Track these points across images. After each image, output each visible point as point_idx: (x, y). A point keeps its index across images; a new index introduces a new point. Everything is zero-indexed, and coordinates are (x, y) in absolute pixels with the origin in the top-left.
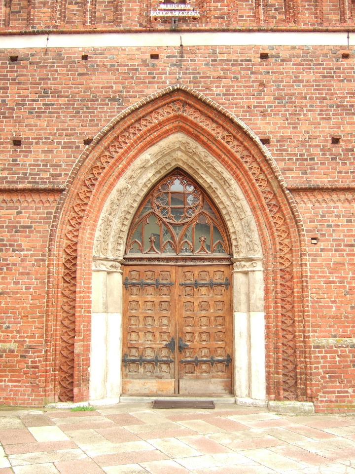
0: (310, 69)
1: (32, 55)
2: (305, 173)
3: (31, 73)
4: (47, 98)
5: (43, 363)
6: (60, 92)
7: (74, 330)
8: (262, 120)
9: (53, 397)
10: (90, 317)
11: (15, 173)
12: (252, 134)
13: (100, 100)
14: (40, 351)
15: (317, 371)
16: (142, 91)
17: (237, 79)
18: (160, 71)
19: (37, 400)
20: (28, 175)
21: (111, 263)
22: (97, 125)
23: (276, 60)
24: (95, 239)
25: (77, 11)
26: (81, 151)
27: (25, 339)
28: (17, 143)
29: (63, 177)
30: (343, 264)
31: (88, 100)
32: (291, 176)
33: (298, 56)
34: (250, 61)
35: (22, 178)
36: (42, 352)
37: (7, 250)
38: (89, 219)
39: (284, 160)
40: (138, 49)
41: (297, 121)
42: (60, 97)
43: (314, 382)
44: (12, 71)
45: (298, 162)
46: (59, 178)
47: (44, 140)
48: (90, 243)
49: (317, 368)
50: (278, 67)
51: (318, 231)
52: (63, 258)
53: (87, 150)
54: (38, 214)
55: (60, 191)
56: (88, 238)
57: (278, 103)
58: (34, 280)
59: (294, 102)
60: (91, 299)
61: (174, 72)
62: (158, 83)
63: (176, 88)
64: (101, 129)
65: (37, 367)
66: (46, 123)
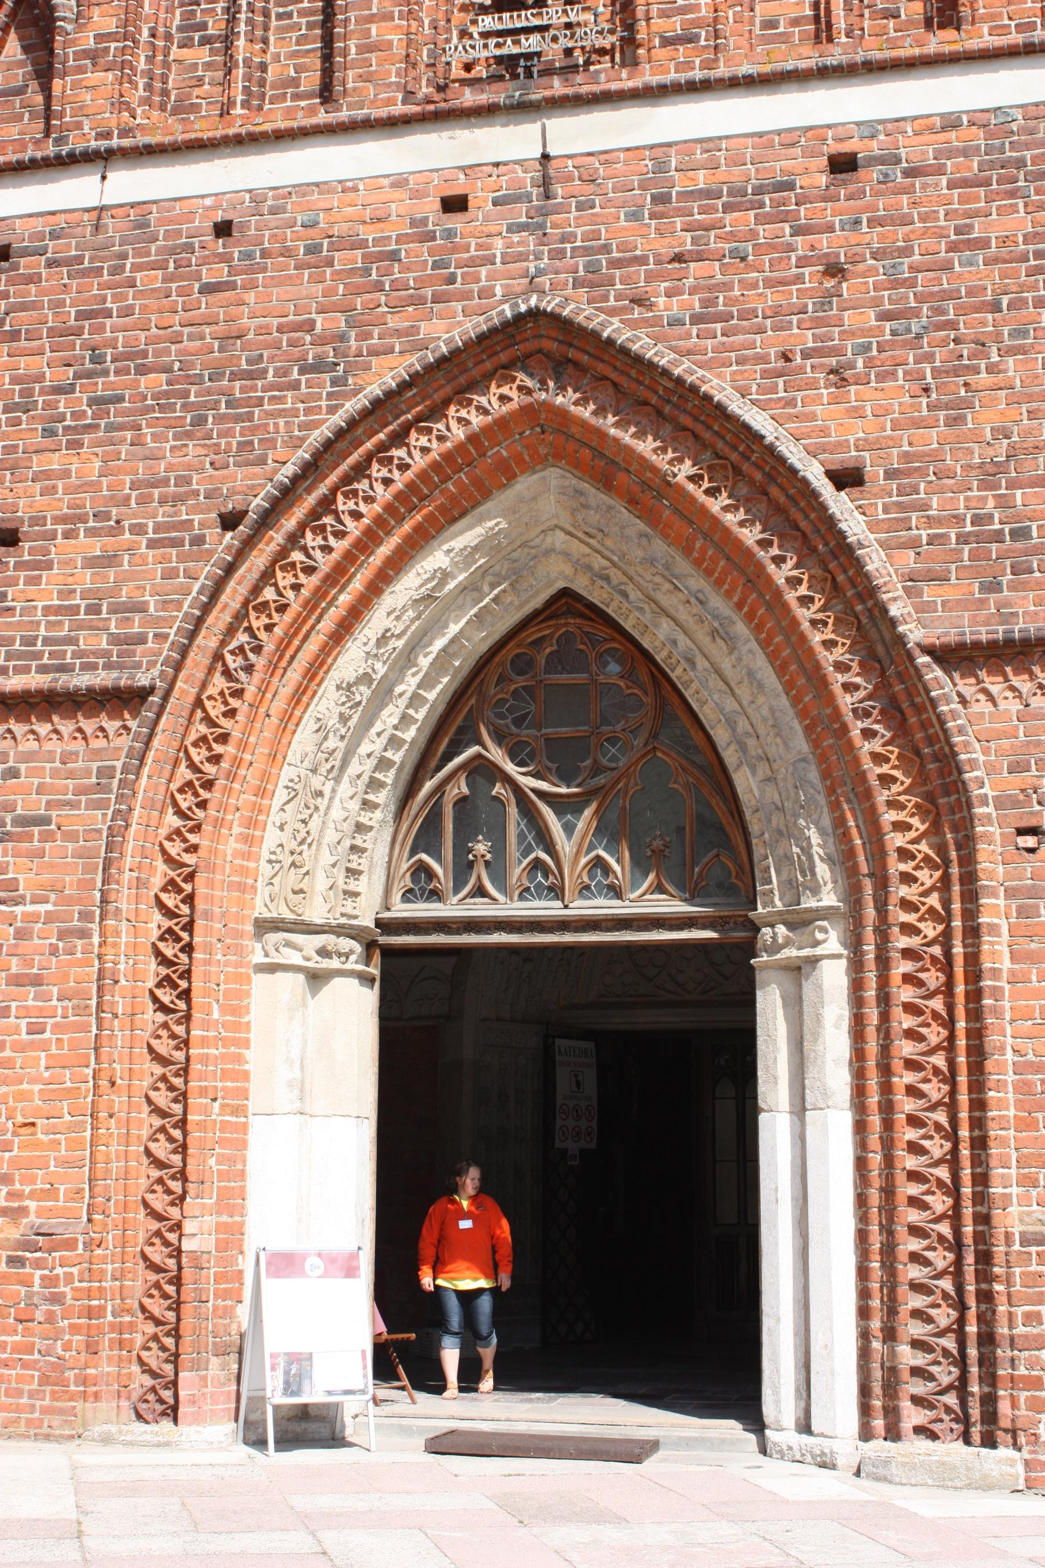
0: (1012, 194)
1: (54, 236)
2: (994, 587)
4: (100, 380)
5: (77, 1284)
6: (144, 354)
7: (182, 1175)
8: (834, 401)
9: (115, 1405)
10: (244, 1128)
12: (793, 454)
13: (271, 372)
14: (71, 1245)
15: (1035, 1331)
17: (743, 259)
18: (473, 252)
19: (61, 1411)
20: (39, 643)
21: (319, 940)
22: (262, 461)
23: (886, 175)
24: (265, 855)
25: (208, 66)
26: (211, 553)
27: (27, 1203)
29: (150, 644)
31: (234, 377)
32: (939, 600)
33: (966, 152)
34: (790, 186)
35: (20, 656)
36: (76, 1248)
38: (236, 786)
39: (914, 544)
40: (399, 182)
41: (963, 393)
42: (142, 370)
43: (1022, 1371)
45: (966, 548)
46: (139, 649)
47: (91, 524)
48: (243, 871)
50: (892, 200)
51: (1039, 803)
52: (153, 925)
53: (229, 548)
54: (71, 775)
56: (236, 853)
57: (894, 333)
58: (55, 1002)
59: (953, 325)
60: (246, 1067)
61: (521, 254)
63: (523, 308)
64: (276, 471)
65: (57, 1299)
66: (98, 464)
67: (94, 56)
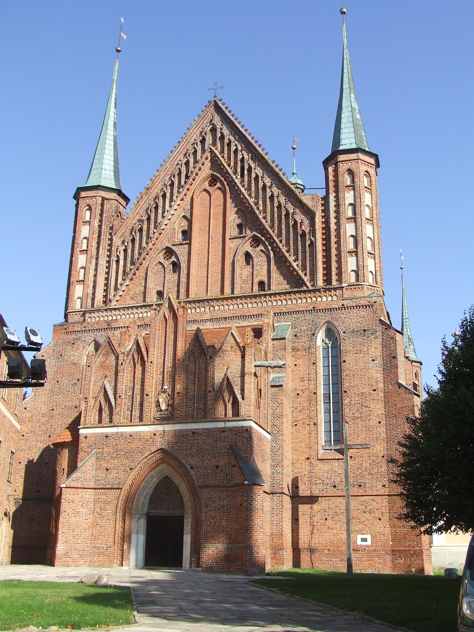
3: (112, 441)
11: (106, 482)
16: (150, 449)
28: (107, 470)
30: (216, 516)
37: (103, 510)
40: (149, 432)
42: (122, 451)
44: (106, 441)
48: (132, 507)
49: (203, 555)
55: (121, 489)
59: (203, 452)
62: (155, 445)
65: (111, 553)
67: (117, 413)
